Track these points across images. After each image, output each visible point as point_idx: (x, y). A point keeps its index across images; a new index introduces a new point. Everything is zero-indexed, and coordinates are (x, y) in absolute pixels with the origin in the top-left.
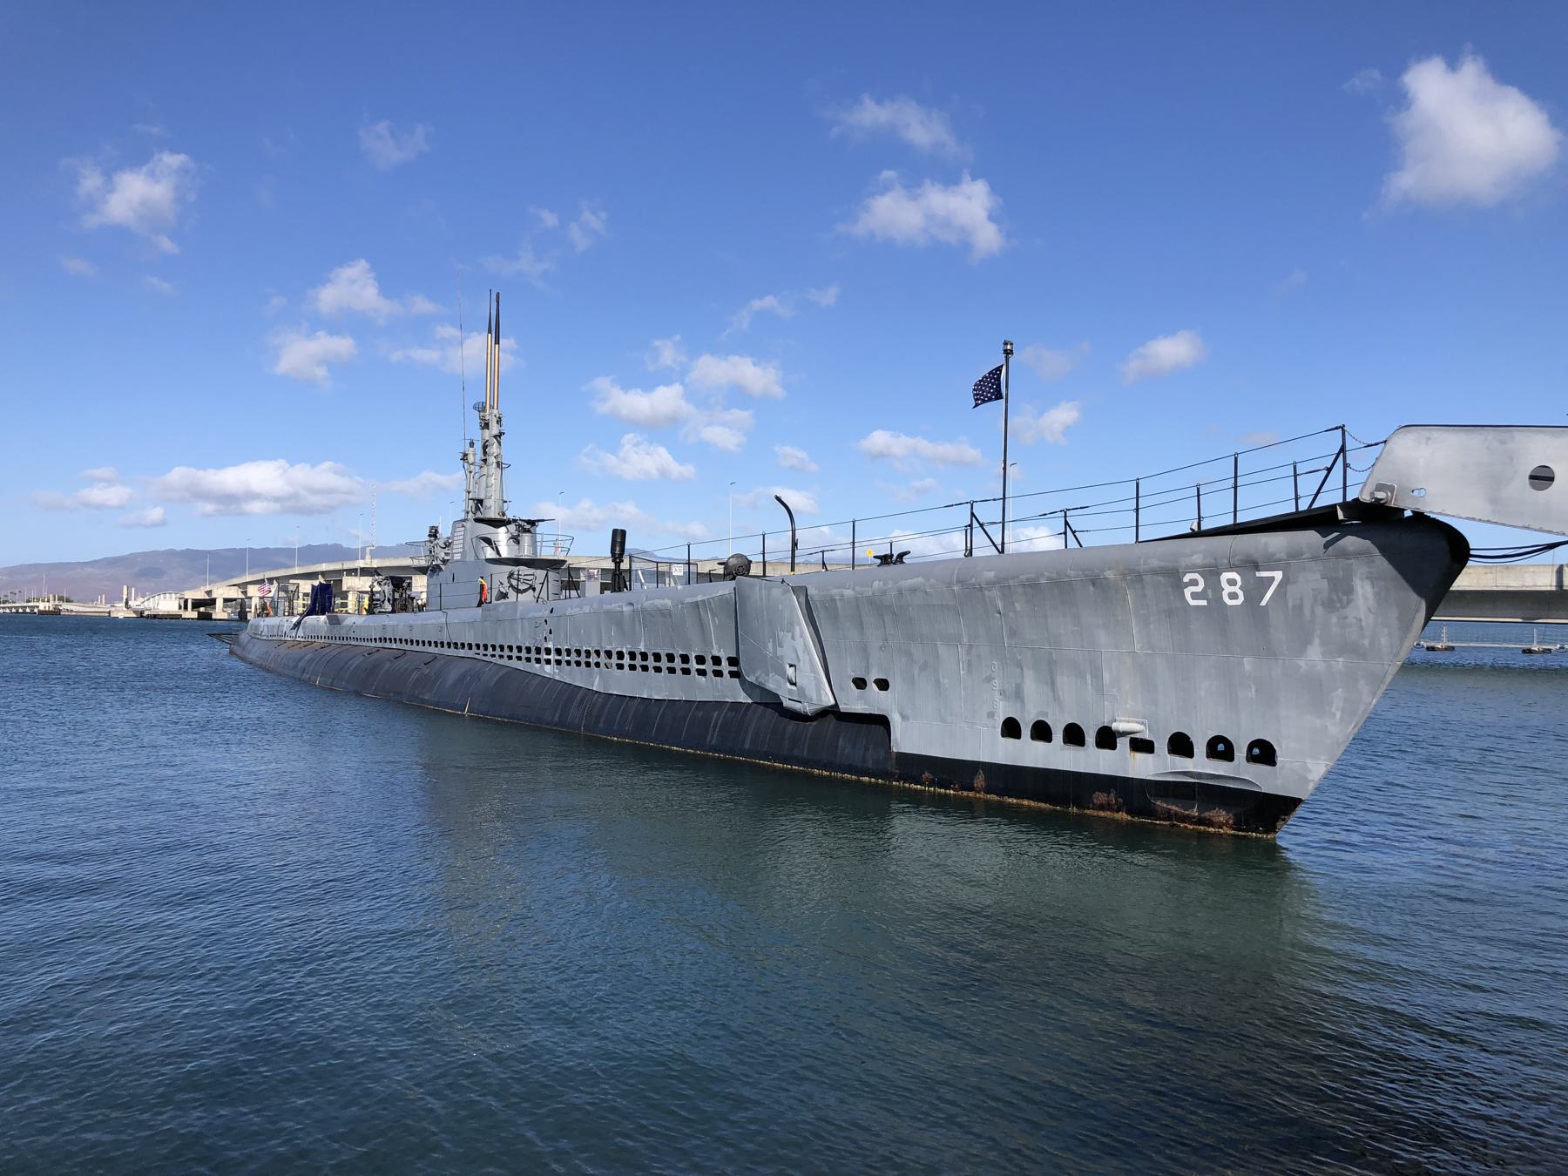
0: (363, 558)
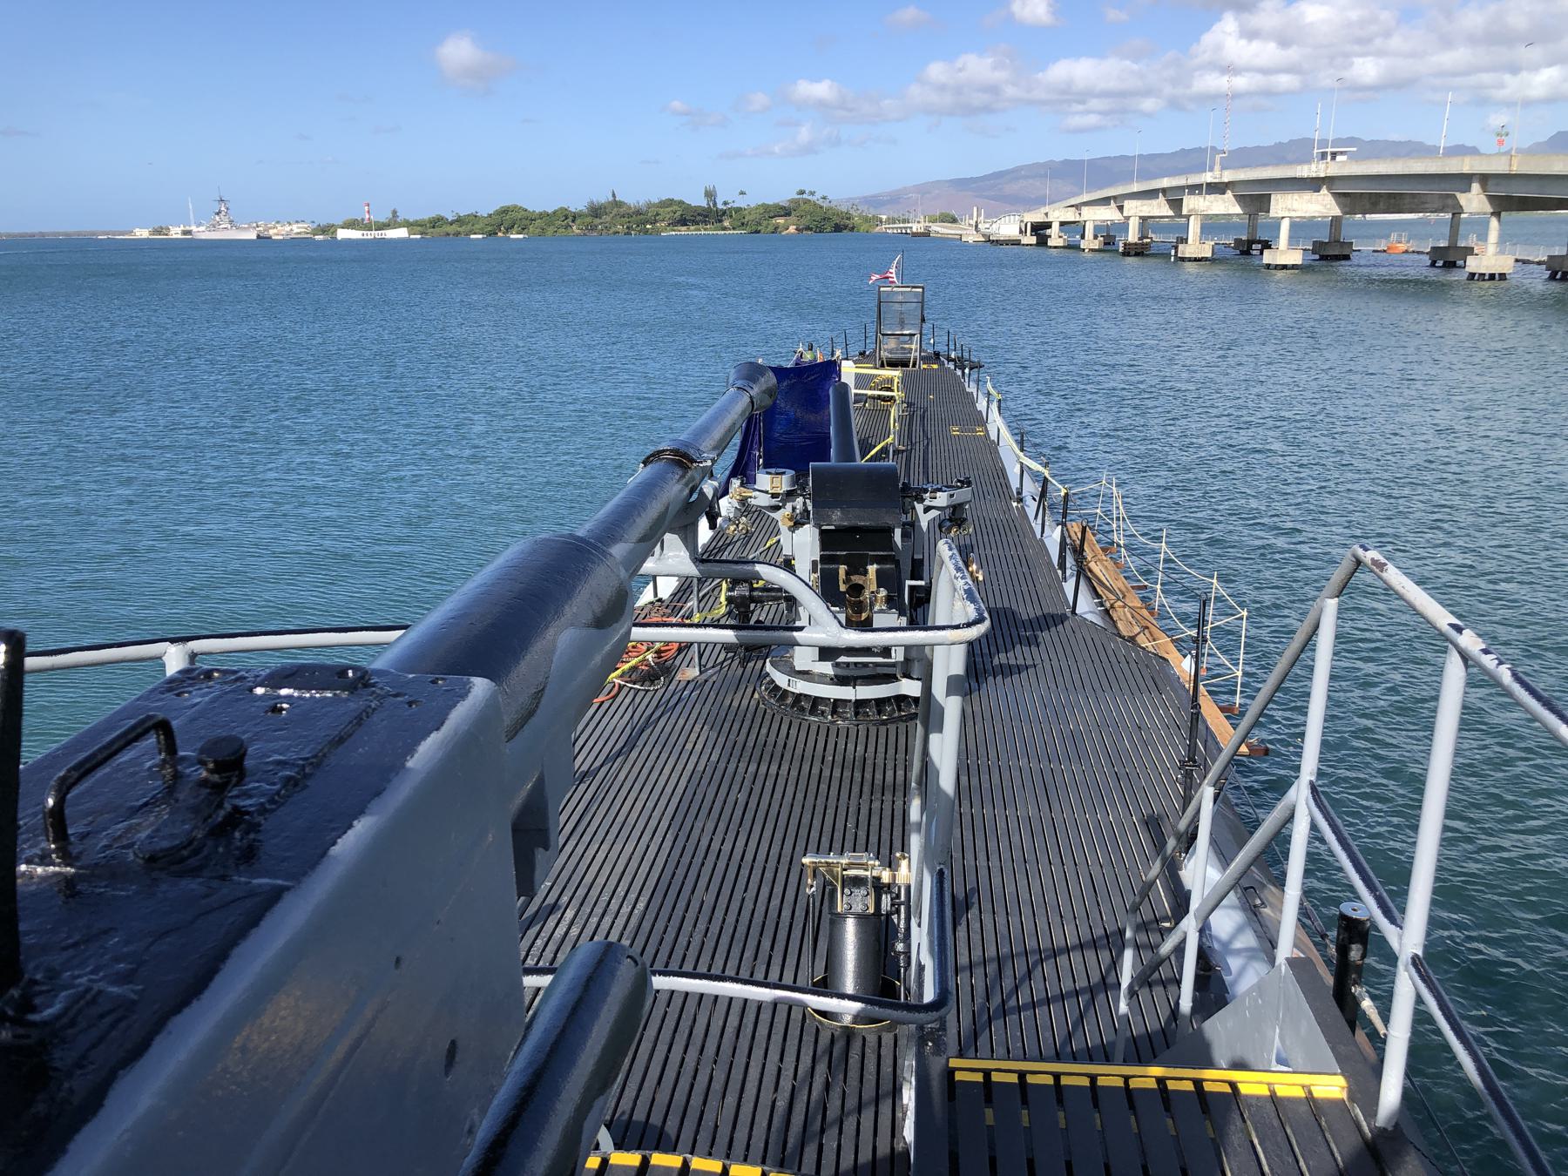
0: (1211, 170)
